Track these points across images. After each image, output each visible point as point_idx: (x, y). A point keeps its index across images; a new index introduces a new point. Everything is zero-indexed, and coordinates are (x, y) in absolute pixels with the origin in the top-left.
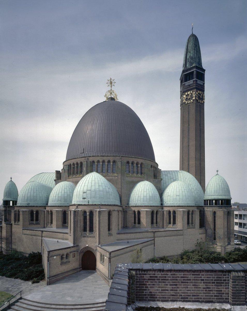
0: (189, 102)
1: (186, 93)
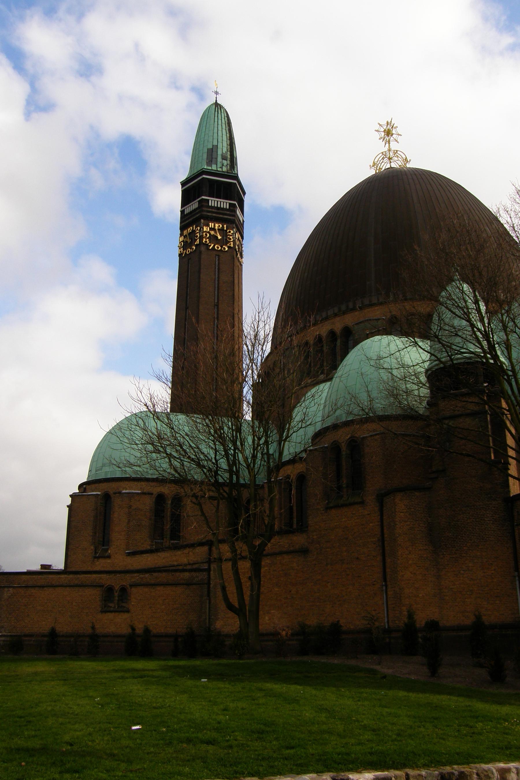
0: (218, 248)
1: (210, 224)
